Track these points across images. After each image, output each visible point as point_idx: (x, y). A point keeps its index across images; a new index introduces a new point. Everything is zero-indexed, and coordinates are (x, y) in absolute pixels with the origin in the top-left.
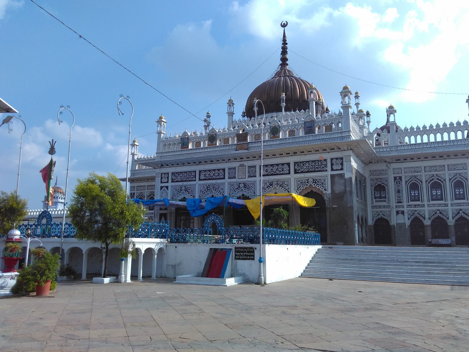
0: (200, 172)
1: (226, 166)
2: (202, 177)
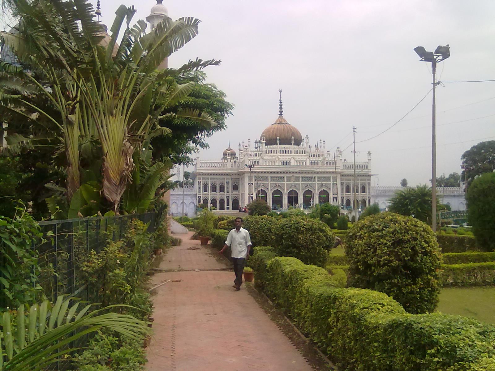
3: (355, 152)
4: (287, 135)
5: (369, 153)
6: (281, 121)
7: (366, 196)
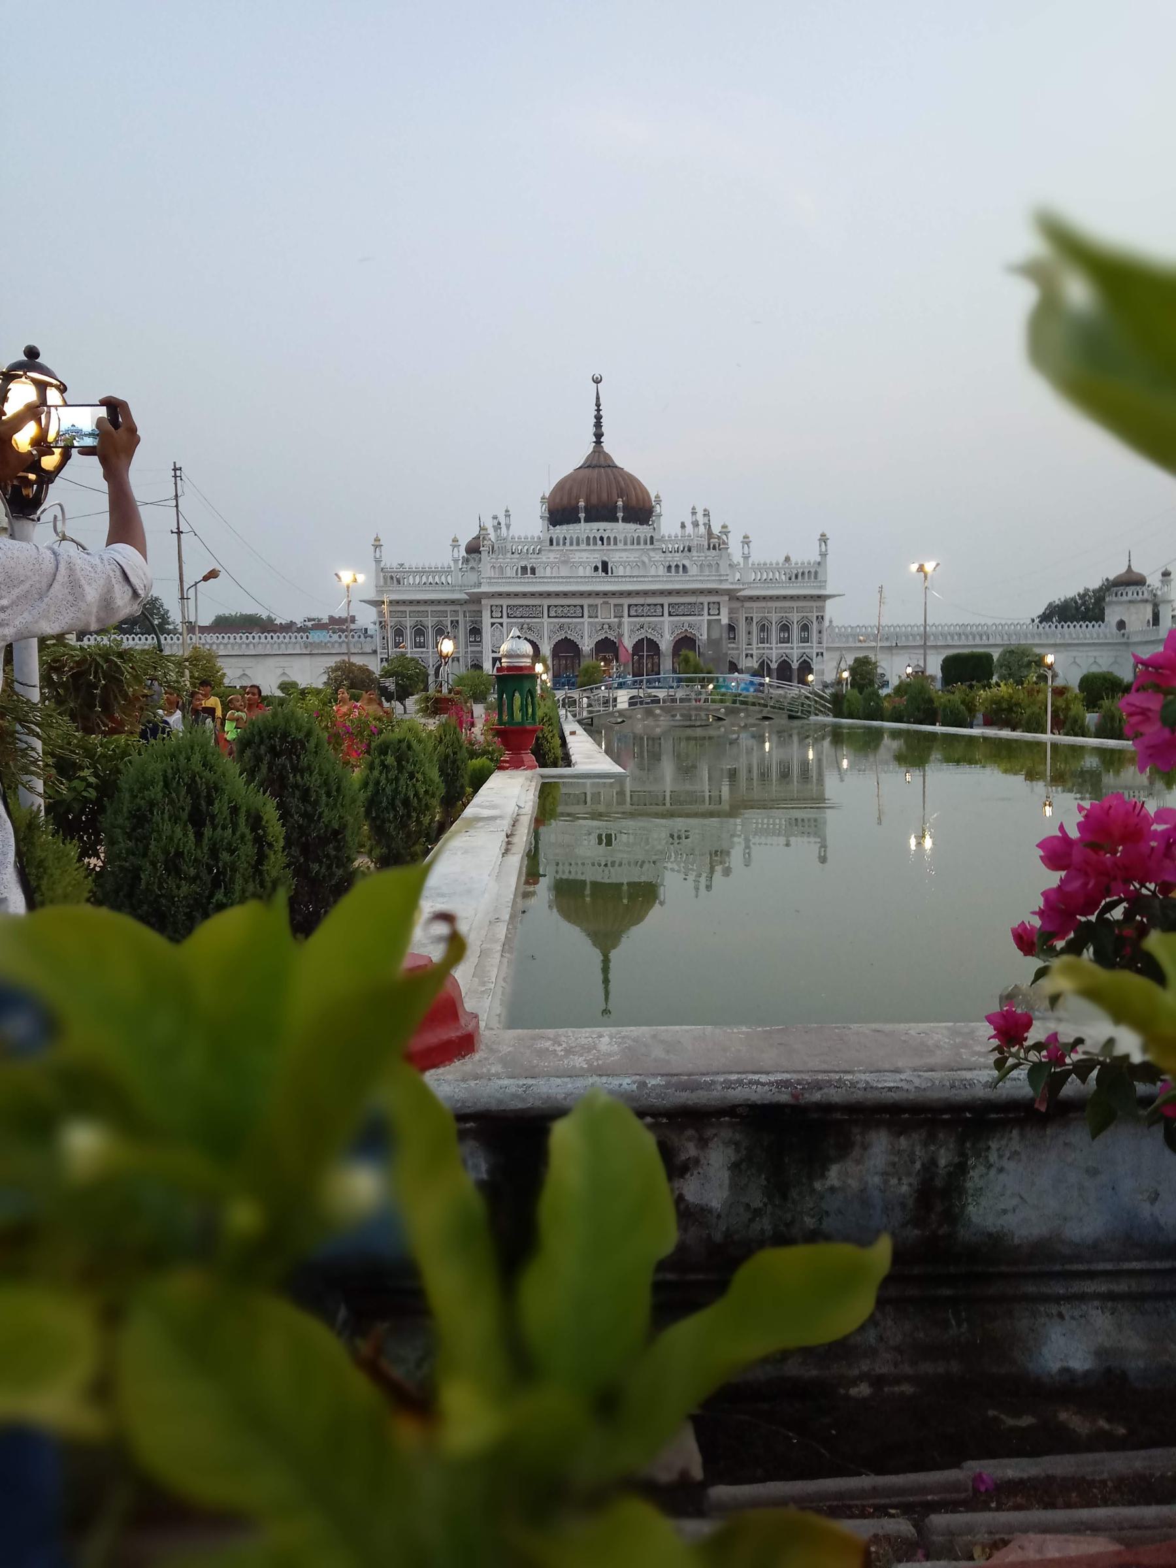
0: (549, 607)
1: (585, 602)
2: (552, 614)
3: (179, 533)
4: (604, 496)
5: (823, 539)
6: (599, 461)
7: (813, 649)
